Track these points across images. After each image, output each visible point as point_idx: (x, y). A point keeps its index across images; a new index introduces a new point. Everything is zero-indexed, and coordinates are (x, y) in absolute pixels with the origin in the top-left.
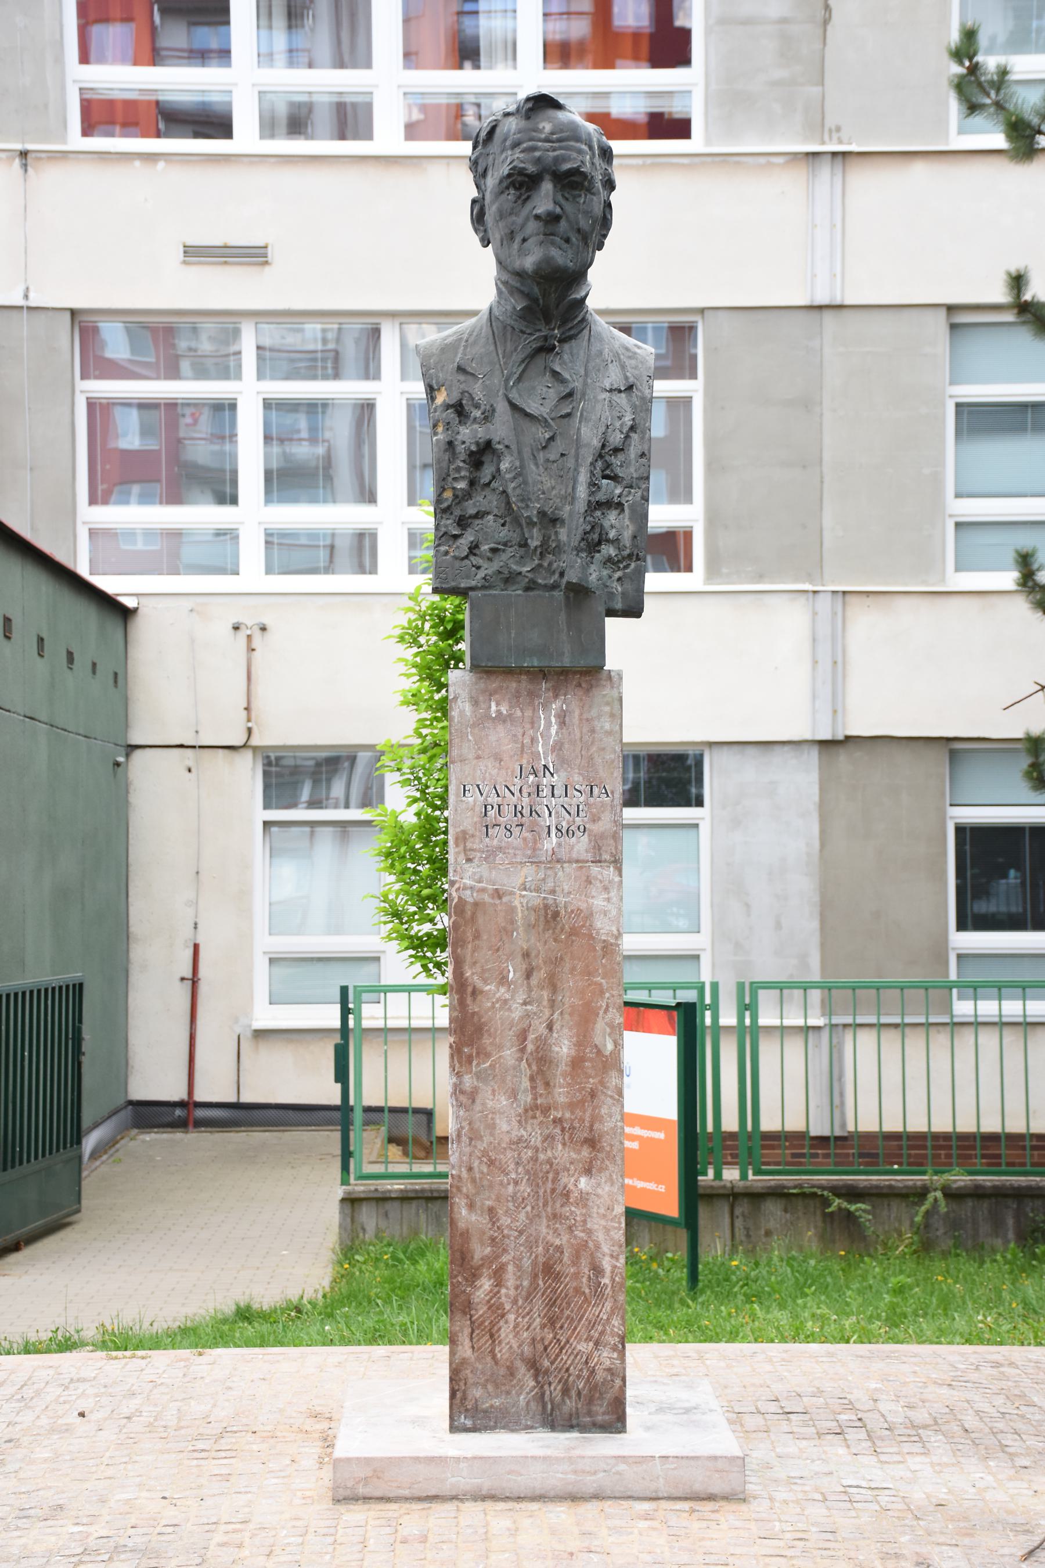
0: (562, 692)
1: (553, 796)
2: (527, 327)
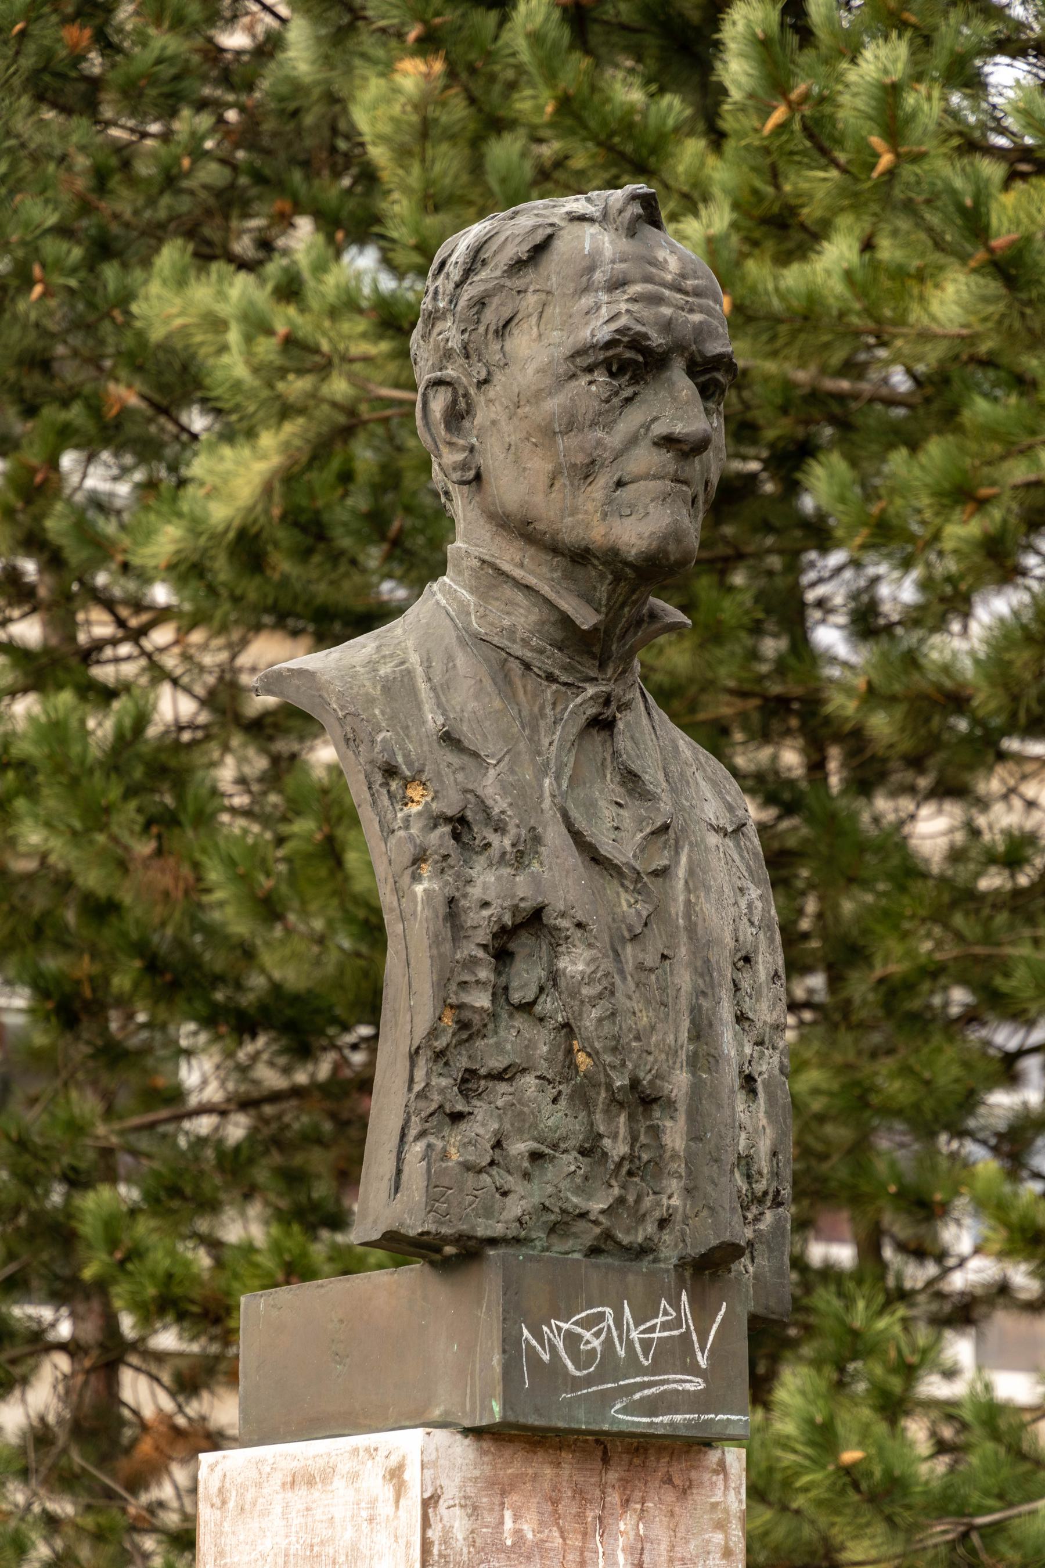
0: (637, 1495)
2: (564, 668)
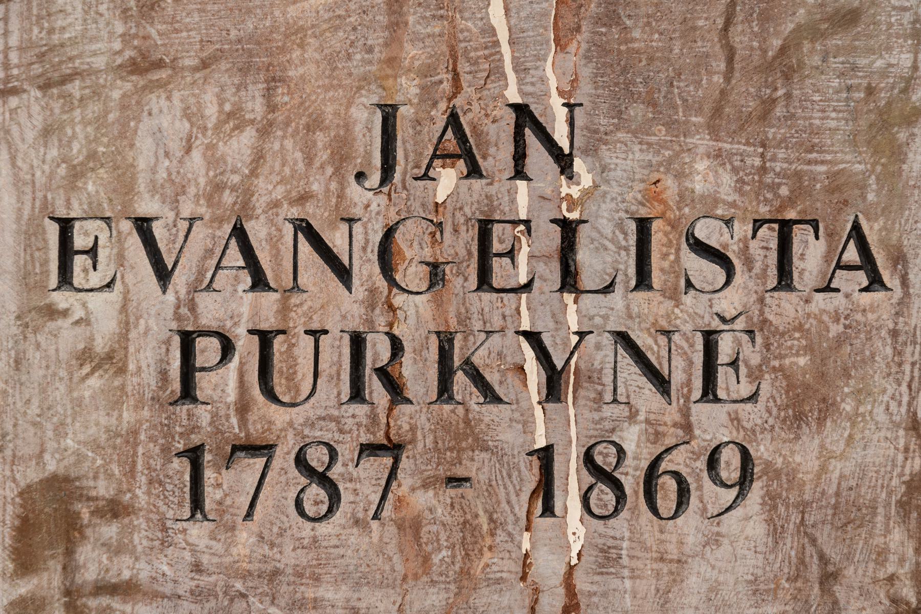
1: (569, 280)
